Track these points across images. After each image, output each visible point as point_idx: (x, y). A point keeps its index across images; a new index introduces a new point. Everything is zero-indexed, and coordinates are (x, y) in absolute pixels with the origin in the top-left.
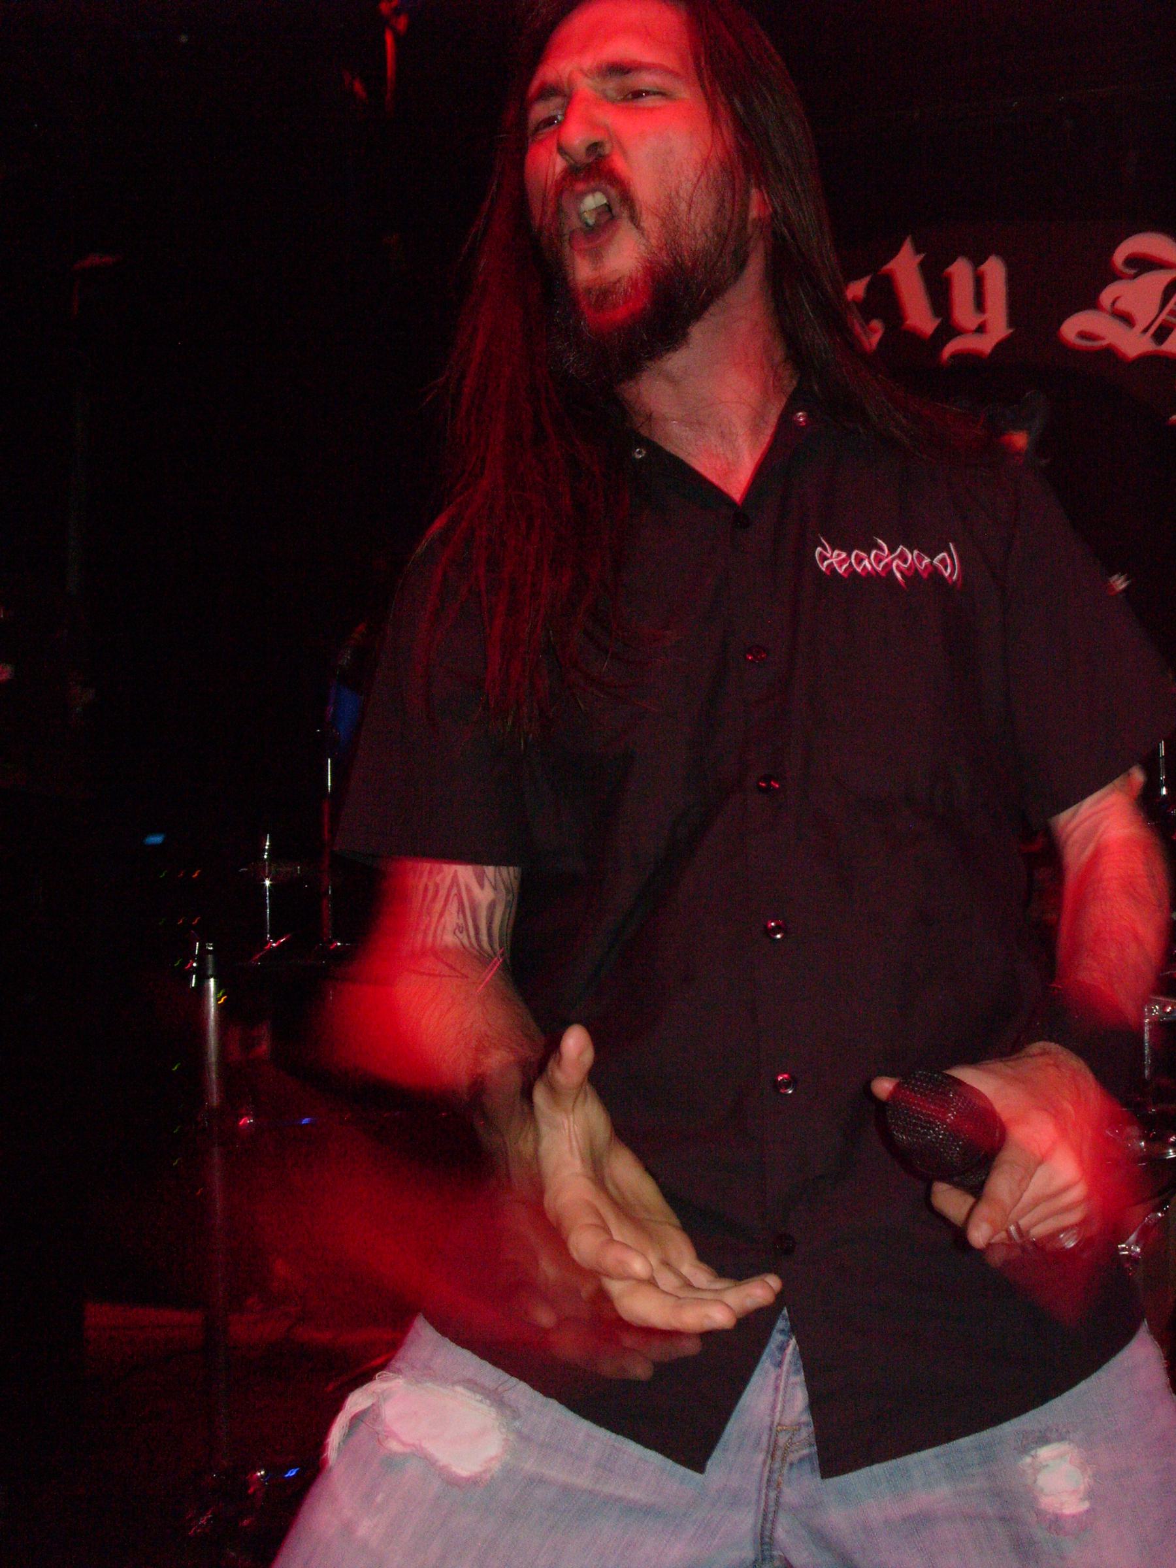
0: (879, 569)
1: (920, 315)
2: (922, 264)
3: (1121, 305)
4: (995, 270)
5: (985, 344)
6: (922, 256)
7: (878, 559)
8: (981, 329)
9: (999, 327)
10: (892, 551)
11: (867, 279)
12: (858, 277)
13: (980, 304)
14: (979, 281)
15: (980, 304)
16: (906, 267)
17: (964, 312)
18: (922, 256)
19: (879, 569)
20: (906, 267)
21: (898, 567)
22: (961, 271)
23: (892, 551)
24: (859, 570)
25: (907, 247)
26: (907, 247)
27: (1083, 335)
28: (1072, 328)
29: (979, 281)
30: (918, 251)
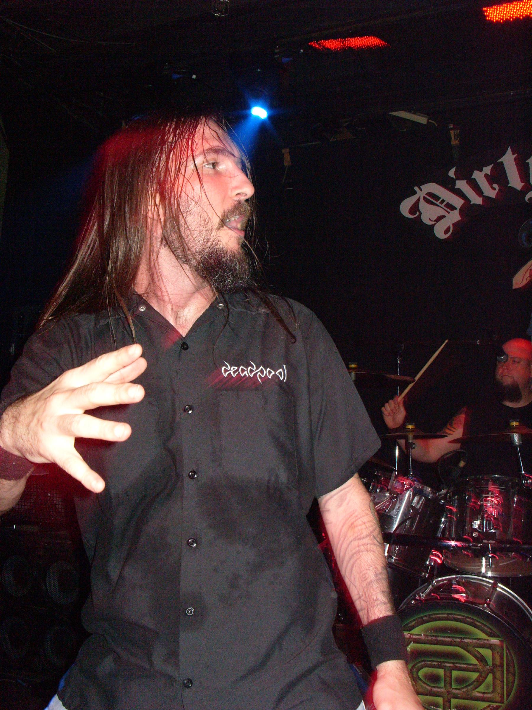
0: (252, 376)
1: (515, 182)
2: (515, 159)
6: (515, 156)
7: (251, 371)
10: (257, 368)
11: (491, 166)
12: (486, 165)
16: (509, 160)
18: (515, 156)
19: (252, 376)
20: (509, 160)
21: (260, 375)
23: (257, 368)
24: (243, 375)
25: (509, 150)
26: (509, 150)
30: (513, 154)
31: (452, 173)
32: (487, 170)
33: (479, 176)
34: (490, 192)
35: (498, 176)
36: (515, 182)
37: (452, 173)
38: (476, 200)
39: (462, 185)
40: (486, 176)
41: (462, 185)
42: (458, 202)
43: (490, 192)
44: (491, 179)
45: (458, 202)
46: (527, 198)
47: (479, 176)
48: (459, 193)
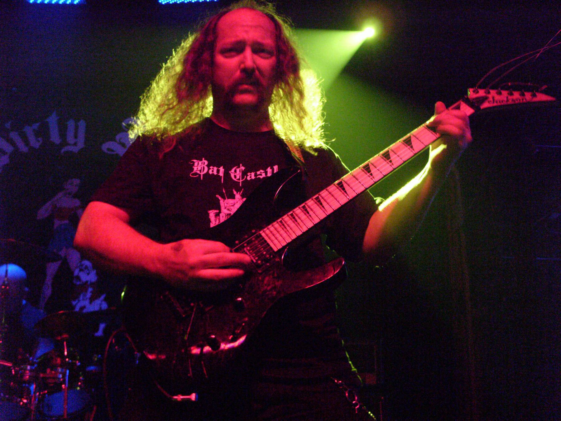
1: (55, 138)
3: (122, 141)
4: (82, 124)
5: (75, 149)
8: (75, 144)
9: (81, 145)
13: (76, 137)
14: (76, 128)
15: (76, 137)
16: (53, 120)
17: (70, 139)
20: (53, 120)
22: (71, 124)
27: (109, 149)
28: (105, 147)
29: (76, 128)
31: (8, 125)
32: (36, 126)
33: (29, 130)
34: (35, 143)
35: (43, 132)
36: (55, 138)
37: (8, 125)
38: (23, 148)
39: (14, 135)
40: (34, 130)
41: (14, 135)
42: (9, 149)
43: (35, 143)
44: (37, 134)
45: (9, 149)
46: (62, 151)
47: (29, 130)
48: (11, 141)
